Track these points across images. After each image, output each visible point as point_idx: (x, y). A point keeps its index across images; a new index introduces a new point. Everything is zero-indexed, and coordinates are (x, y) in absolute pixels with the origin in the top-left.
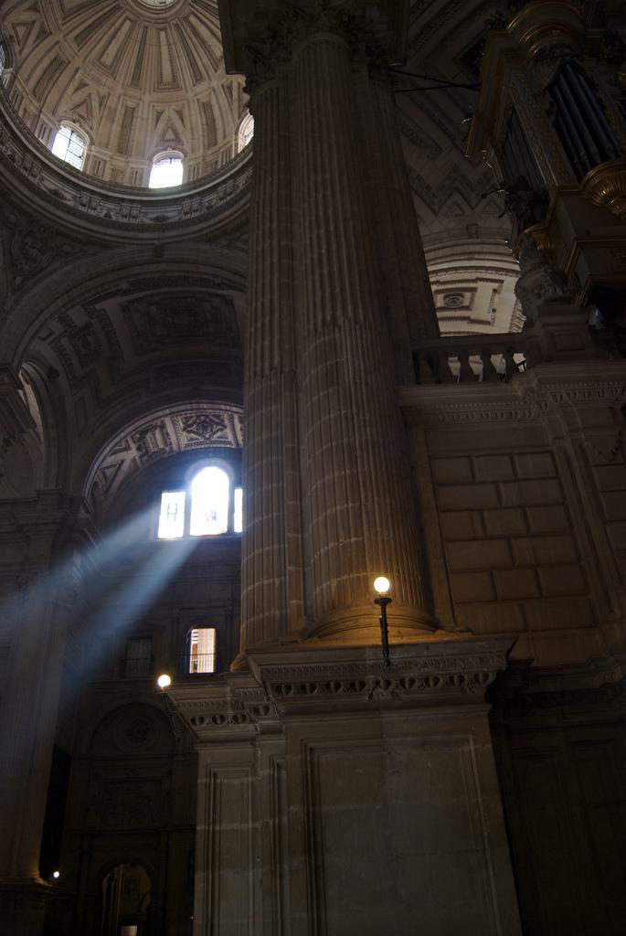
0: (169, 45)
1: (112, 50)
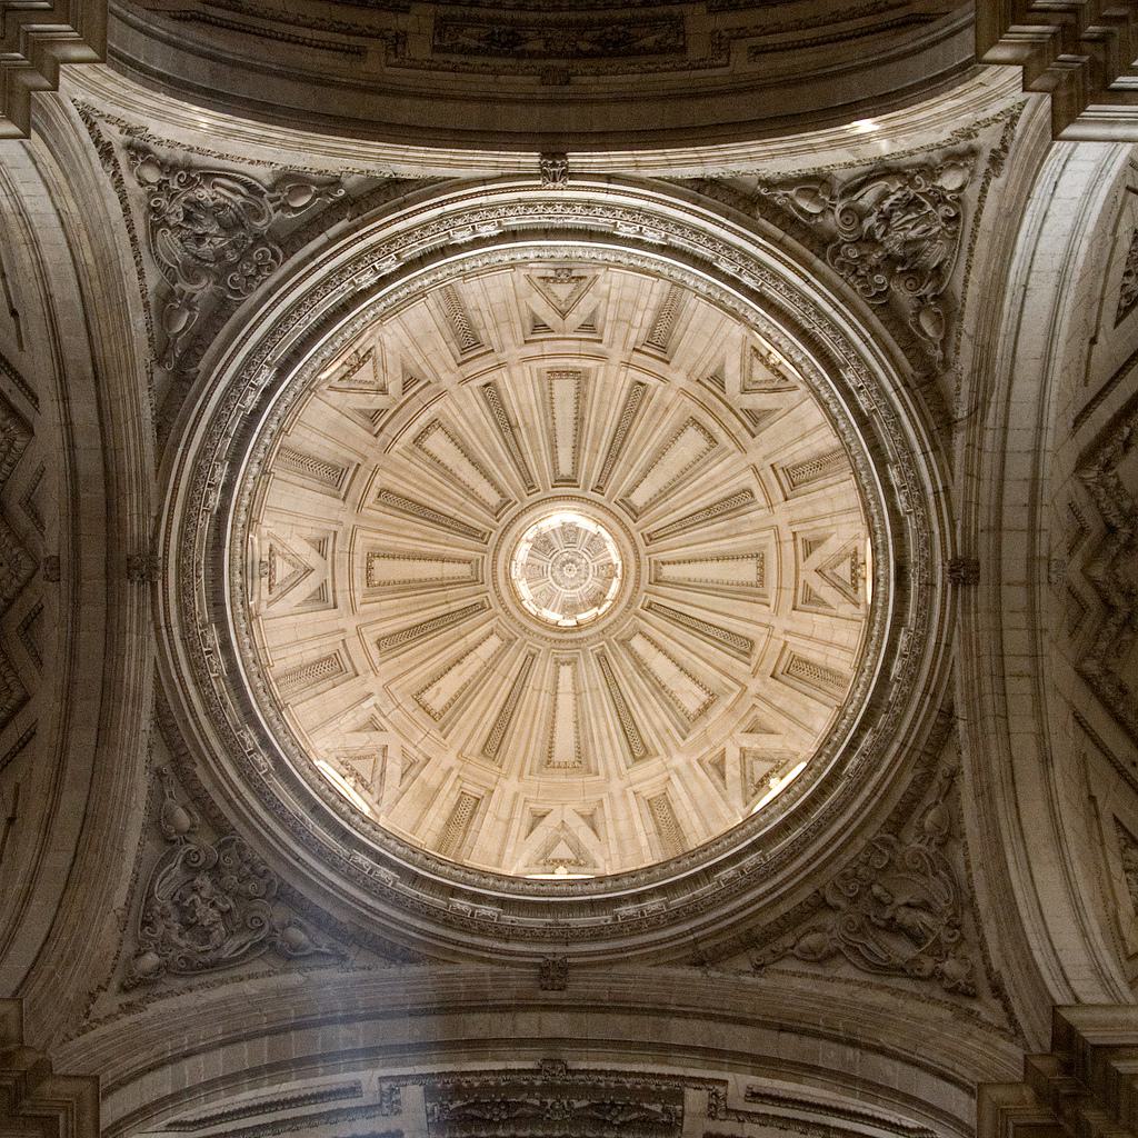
0: (577, 694)
1: (451, 684)
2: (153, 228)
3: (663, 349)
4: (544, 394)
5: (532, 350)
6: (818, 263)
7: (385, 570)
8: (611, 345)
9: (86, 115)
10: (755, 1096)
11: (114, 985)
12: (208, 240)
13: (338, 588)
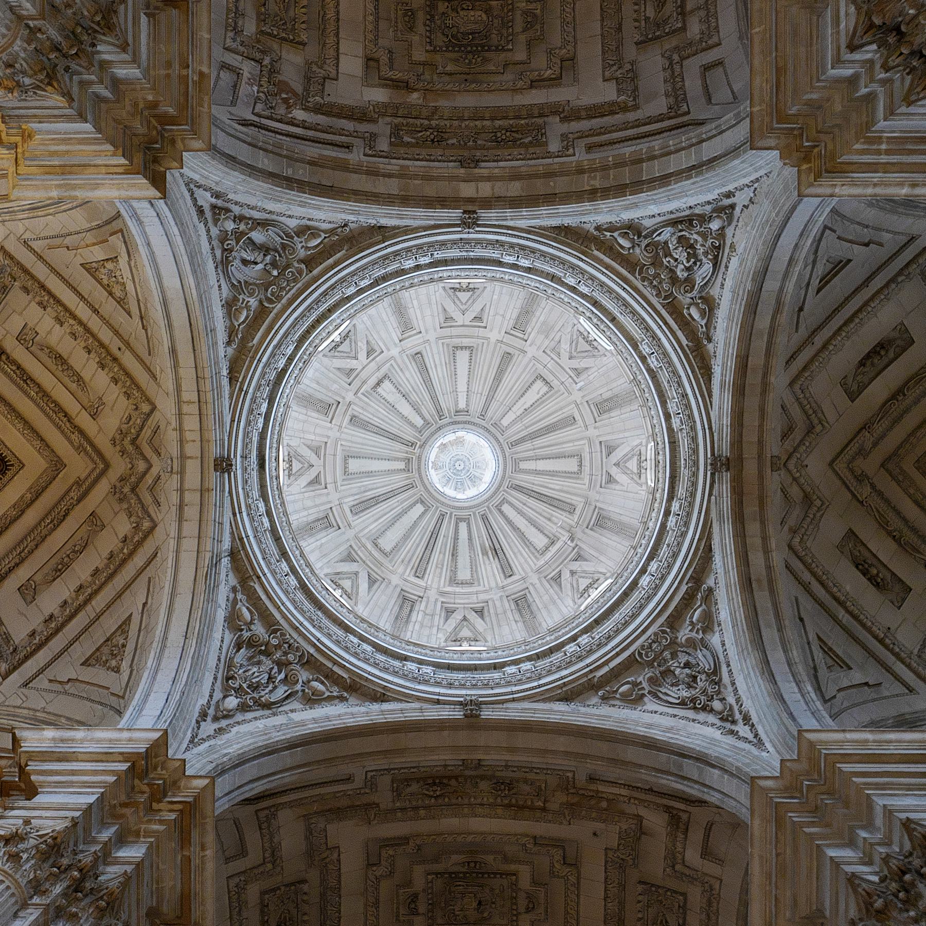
1: (531, 397)
2: (716, 671)
3: (405, 598)
4: (476, 571)
5: (482, 597)
6: (312, 651)
7: (571, 465)
8: (437, 600)
9: (759, 744)
10: (348, 147)
11: (738, 209)
12: (682, 665)
13: (599, 454)
